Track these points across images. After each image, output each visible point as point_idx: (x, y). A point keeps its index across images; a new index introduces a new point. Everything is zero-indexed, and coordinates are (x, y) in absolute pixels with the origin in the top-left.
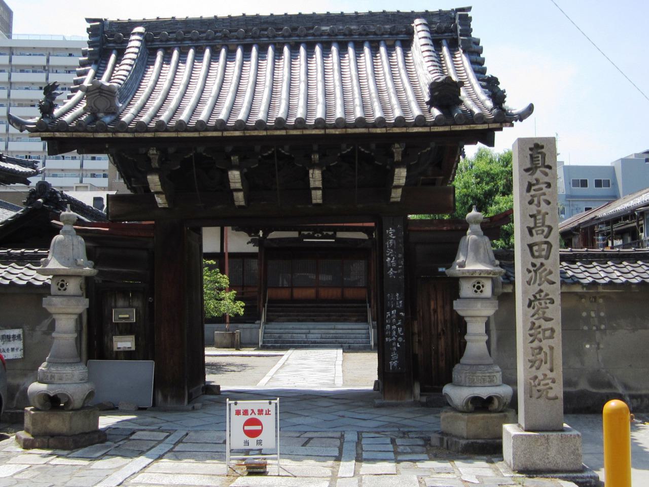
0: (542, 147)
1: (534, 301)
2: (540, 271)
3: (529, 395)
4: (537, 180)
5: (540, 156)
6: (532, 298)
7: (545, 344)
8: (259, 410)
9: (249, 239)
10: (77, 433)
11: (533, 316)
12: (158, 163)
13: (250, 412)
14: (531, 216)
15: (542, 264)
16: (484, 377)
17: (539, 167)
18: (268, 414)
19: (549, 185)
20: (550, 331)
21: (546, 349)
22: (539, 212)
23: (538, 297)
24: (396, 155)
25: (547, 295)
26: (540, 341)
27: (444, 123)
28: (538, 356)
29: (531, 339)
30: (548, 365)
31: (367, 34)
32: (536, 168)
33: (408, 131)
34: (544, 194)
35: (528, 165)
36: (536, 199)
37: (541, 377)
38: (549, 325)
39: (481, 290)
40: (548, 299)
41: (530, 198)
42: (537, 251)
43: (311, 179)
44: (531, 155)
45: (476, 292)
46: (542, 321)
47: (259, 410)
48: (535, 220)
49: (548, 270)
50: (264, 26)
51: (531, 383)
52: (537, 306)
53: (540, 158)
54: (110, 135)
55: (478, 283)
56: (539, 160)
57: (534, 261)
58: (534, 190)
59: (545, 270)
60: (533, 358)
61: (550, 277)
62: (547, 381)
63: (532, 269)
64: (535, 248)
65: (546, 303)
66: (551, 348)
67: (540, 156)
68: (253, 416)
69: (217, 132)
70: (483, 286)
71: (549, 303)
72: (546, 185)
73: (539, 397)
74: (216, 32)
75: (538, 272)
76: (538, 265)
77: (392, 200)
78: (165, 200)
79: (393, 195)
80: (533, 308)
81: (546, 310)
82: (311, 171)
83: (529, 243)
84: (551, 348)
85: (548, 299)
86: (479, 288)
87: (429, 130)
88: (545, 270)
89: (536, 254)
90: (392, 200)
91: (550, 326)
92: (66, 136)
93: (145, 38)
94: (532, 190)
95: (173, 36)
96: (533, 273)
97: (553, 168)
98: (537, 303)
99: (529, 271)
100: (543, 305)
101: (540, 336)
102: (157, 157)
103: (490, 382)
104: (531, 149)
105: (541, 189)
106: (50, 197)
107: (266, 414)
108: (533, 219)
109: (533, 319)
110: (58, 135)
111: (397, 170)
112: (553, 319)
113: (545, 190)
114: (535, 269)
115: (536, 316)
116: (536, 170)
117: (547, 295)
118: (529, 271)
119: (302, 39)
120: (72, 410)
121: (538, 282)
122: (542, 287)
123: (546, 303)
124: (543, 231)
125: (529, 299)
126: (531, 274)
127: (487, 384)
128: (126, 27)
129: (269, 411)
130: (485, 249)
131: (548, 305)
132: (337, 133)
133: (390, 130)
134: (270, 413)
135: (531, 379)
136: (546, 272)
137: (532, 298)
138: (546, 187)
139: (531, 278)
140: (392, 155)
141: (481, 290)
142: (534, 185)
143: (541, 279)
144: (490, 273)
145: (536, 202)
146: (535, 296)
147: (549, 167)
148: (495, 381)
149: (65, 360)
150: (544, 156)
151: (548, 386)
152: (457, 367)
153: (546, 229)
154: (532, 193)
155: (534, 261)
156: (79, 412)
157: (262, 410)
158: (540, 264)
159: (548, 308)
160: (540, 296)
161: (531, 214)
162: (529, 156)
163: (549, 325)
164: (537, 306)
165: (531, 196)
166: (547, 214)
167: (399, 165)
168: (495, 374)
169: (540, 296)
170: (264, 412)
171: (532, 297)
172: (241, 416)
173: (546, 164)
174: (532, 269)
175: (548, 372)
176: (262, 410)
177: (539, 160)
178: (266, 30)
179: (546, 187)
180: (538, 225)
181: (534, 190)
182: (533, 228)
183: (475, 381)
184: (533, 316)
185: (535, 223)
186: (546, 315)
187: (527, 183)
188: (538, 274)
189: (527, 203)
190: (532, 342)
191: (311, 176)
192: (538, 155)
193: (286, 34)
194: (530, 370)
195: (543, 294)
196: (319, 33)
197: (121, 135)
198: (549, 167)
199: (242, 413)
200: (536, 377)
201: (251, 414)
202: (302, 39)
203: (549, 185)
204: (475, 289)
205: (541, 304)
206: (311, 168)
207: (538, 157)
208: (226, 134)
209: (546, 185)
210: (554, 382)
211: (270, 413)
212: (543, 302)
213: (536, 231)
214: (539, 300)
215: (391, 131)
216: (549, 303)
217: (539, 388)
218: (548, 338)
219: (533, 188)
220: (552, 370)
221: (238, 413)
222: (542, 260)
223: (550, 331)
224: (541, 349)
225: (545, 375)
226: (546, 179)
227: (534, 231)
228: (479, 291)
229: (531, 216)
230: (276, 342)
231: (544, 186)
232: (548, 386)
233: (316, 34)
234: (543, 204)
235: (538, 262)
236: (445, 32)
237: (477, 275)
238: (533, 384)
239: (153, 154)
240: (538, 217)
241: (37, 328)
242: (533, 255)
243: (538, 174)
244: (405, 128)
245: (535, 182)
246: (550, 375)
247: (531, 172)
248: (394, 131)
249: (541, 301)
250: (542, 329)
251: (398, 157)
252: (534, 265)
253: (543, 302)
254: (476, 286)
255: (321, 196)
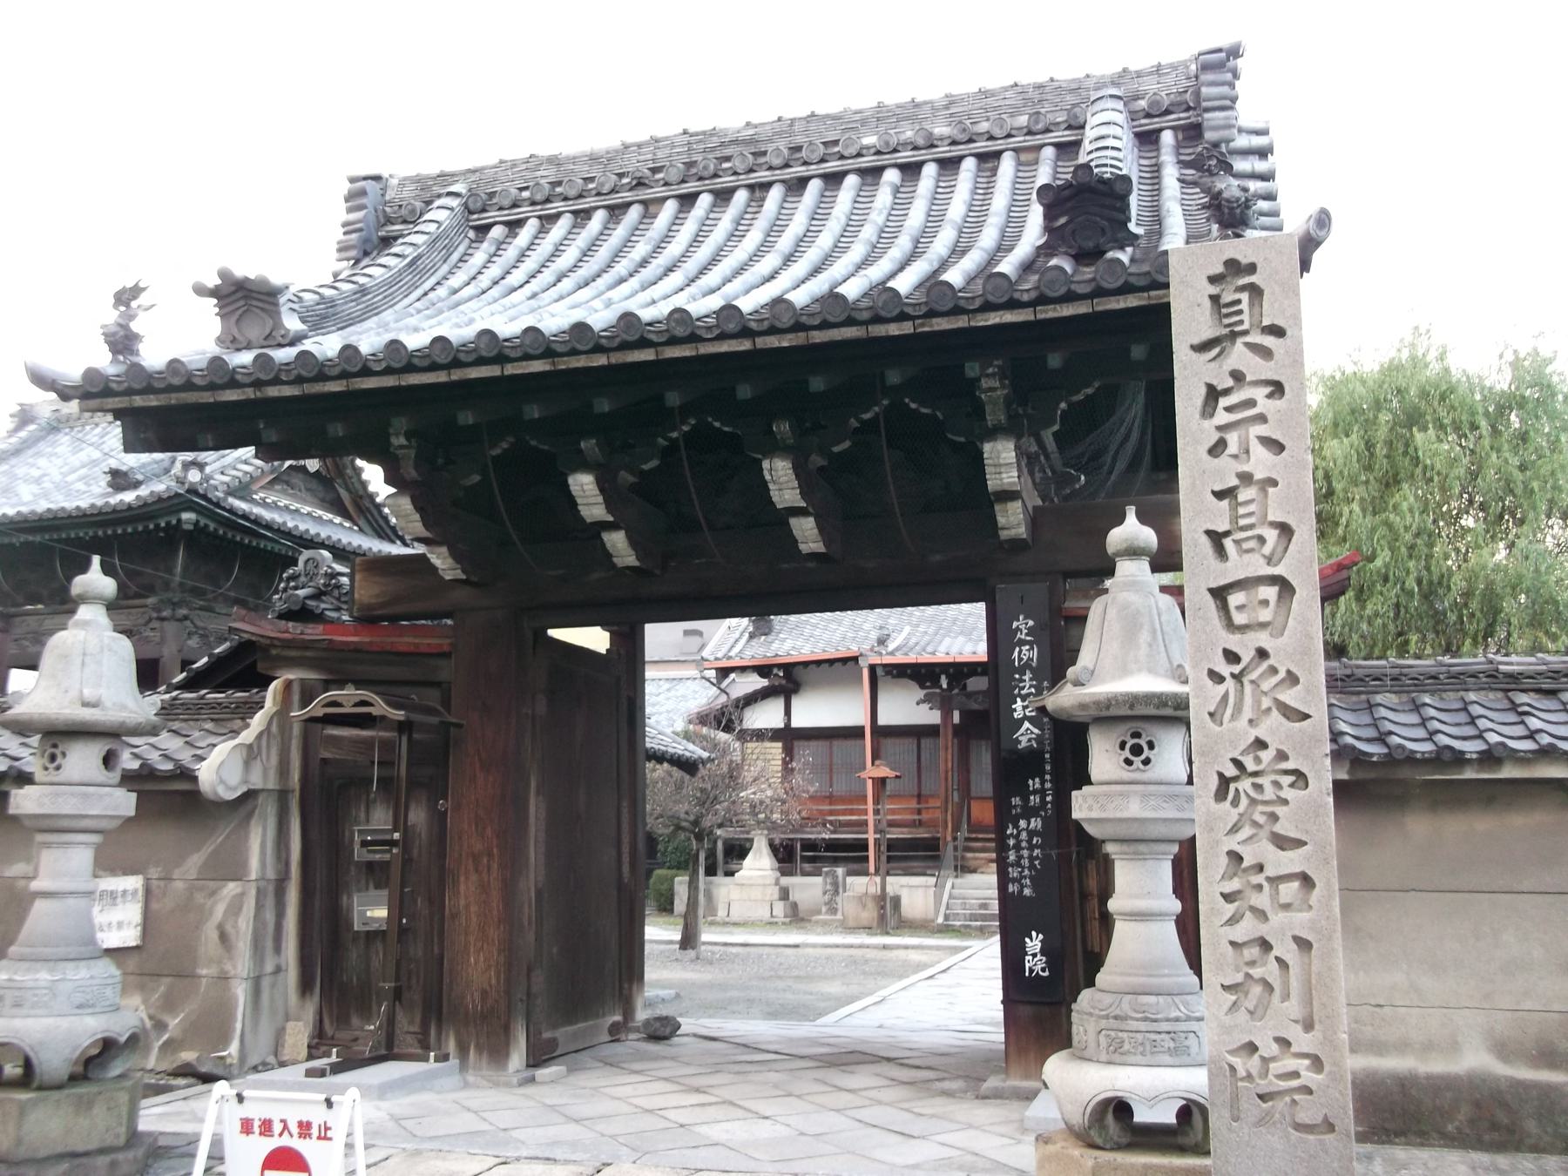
0: (1252, 268)
1: (1235, 779)
2: (1254, 676)
3: (1227, 1114)
4: (1238, 376)
5: (1245, 297)
6: (1231, 771)
7: (1280, 927)
8: (300, 1124)
9: (921, 694)
10: (42, 1153)
11: (1235, 829)
12: (416, 467)
13: (277, 1127)
14: (1219, 495)
15: (1262, 654)
16: (1153, 1036)
17: (1245, 333)
18: (326, 1138)
19: (1277, 389)
20: (1296, 884)
21: (1284, 948)
22: (1246, 478)
23: (1251, 766)
24: (988, 409)
25: (1282, 756)
26: (1261, 915)
27: (1063, 290)
28: (1257, 972)
29: (1230, 909)
30: (1294, 1008)
31: (971, 141)
32: (1234, 336)
33: (973, 324)
34: (1262, 418)
35: (1208, 333)
36: (1233, 438)
37: (1269, 1048)
38: (1290, 861)
39: (1143, 757)
40: (1286, 772)
41: (1215, 436)
42: (1240, 608)
43: (771, 486)
44: (1215, 299)
45: (1128, 762)
46: (1263, 850)
47: (300, 1124)
48: (1236, 505)
49: (1282, 674)
50: (727, 152)
51: (1232, 1068)
52: (1248, 795)
53: (1244, 306)
54: (250, 393)
55: (1137, 735)
56: (1240, 312)
57: (1234, 642)
58: (1228, 409)
59: (1274, 670)
60: (1239, 978)
61: (1290, 697)
62: (1291, 1064)
63: (1225, 669)
64: (1235, 599)
65: (1277, 784)
66: (1303, 944)
67: (1245, 297)
68: (286, 1141)
69: (484, 368)
70: (1151, 746)
71: (1292, 785)
72: (1268, 390)
73: (1263, 1121)
74: (621, 176)
75: (1246, 680)
76: (1247, 656)
77: (1004, 535)
78: (450, 561)
79: (1001, 520)
80: (1235, 803)
81: (1280, 810)
82: (766, 464)
83: (1214, 585)
84: (1303, 944)
85: (1286, 772)
86: (1137, 751)
87: (1032, 318)
88: (1274, 670)
89: (1239, 618)
90: (1004, 535)
91: (1297, 869)
92: (155, 403)
93: (466, 205)
94: (1220, 412)
95: (526, 194)
96: (1230, 684)
97: (1289, 333)
98: (1245, 785)
99: (1216, 677)
100: (1269, 793)
101: (1262, 900)
102: (412, 453)
103: (1173, 1052)
104: (1213, 280)
105: (1251, 403)
106: (325, 585)
107: (319, 1138)
108: (1225, 503)
109: (1232, 843)
110: (138, 401)
111: (987, 448)
112: (1305, 843)
113: (1264, 405)
114: (1237, 669)
115: (1246, 832)
116: (1233, 341)
117: (1282, 756)
118: (1216, 677)
119: (813, 169)
120: (40, 1088)
121: (1247, 713)
122: (1261, 732)
123: (1277, 784)
124: (1262, 540)
125: (1221, 775)
126: (1221, 689)
127: (1167, 1059)
128: (429, 189)
129: (327, 1129)
130: (1154, 632)
131: (1287, 793)
132: (785, 344)
133: (923, 325)
134: (329, 1134)
135: (1231, 1052)
136: (1275, 680)
137: (1231, 771)
138: (1270, 396)
139: (1225, 697)
140: (979, 410)
141: (1143, 757)
142: (1227, 392)
143: (1258, 703)
144: (1165, 705)
145: (1233, 447)
146: (1237, 763)
147: (1277, 331)
148: (1194, 1050)
149: (62, 951)
150: (1255, 291)
151: (1295, 1083)
152: (1085, 995)
153: (1271, 535)
154: (1222, 417)
155: (1234, 642)
156: (55, 1095)
157: (309, 1125)
158: (1253, 653)
159: (1285, 802)
160: (1258, 760)
161: (1217, 488)
162: (1207, 303)
163: (1290, 861)
164: (1248, 795)
165: (1219, 428)
166: (1274, 483)
167: (993, 434)
168: (1194, 1026)
169: (1258, 760)
170: (315, 1132)
171: (1231, 765)
172: (255, 1138)
173: (1266, 323)
174: (1225, 669)
175: (1295, 1033)
176: (309, 1125)
177: (1240, 312)
178: (728, 159)
179: (1270, 396)
180: (1242, 522)
181: (1228, 409)
182: (1227, 534)
183: (1126, 1047)
184: (1235, 829)
185: (1235, 518)
186: (1279, 828)
187: (1203, 390)
188: (1248, 688)
189: (1205, 456)
190: (1233, 920)
191: (768, 477)
192: (1237, 296)
193: (777, 162)
194: (1228, 1020)
195: (1267, 756)
196: (853, 150)
197: (273, 392)
198: (1277, 331)
199: (256, 1129)
200: (1252, 1048)
201: (281, 1135)
202: (813, 169)
203: (1277, 389)
204: (1127, 753)
205: (1258, 787)
206: (765, 456)
207: (1239, 302)
208: (510, 369)
209: (1268, 390)
210: (1317, 1063)
211: (329, 1134)
212: (1265, 781)
213: (1237, 542)
214: (1256, 774)
215: (926, 329)
216: (1292, 785)
217: (1263, 1085)
218: (1286, 907)
219: (1224, 402)
220: (1309, 1026)
221: (246, 1126)
222: (1263, 639)
223: (1296, 884)
224: (1265, 945)
225: (1284, 1043)
226: (1267, 370)
227: (1228, 543)
228: (1137, 760)
229: (1219, 495)
230: (974, 917)
231: (1259, 394)
232: (1295, 1083)
233: (846, 154)
234: (1258, 451)
235: (1245, 646)
236: (1167, 112)
237: (1125, 711)
238: (1242, 1073)
239: (402, 447)
240: (1241, 498)
241: (176, 874)
242: (1230, 626)
243: (1239, 356)
244: (966, 317)
245: (1230, 383)
246: (1303, 1041)
247: (1216, 351)
248: (936, 328)
249: (1259, 780)
250: (1269, 879)
251: (995, 415)
252: (1232, 657)
253: (1265, 781)
254: (1128, 746)
255: (816, 531)
